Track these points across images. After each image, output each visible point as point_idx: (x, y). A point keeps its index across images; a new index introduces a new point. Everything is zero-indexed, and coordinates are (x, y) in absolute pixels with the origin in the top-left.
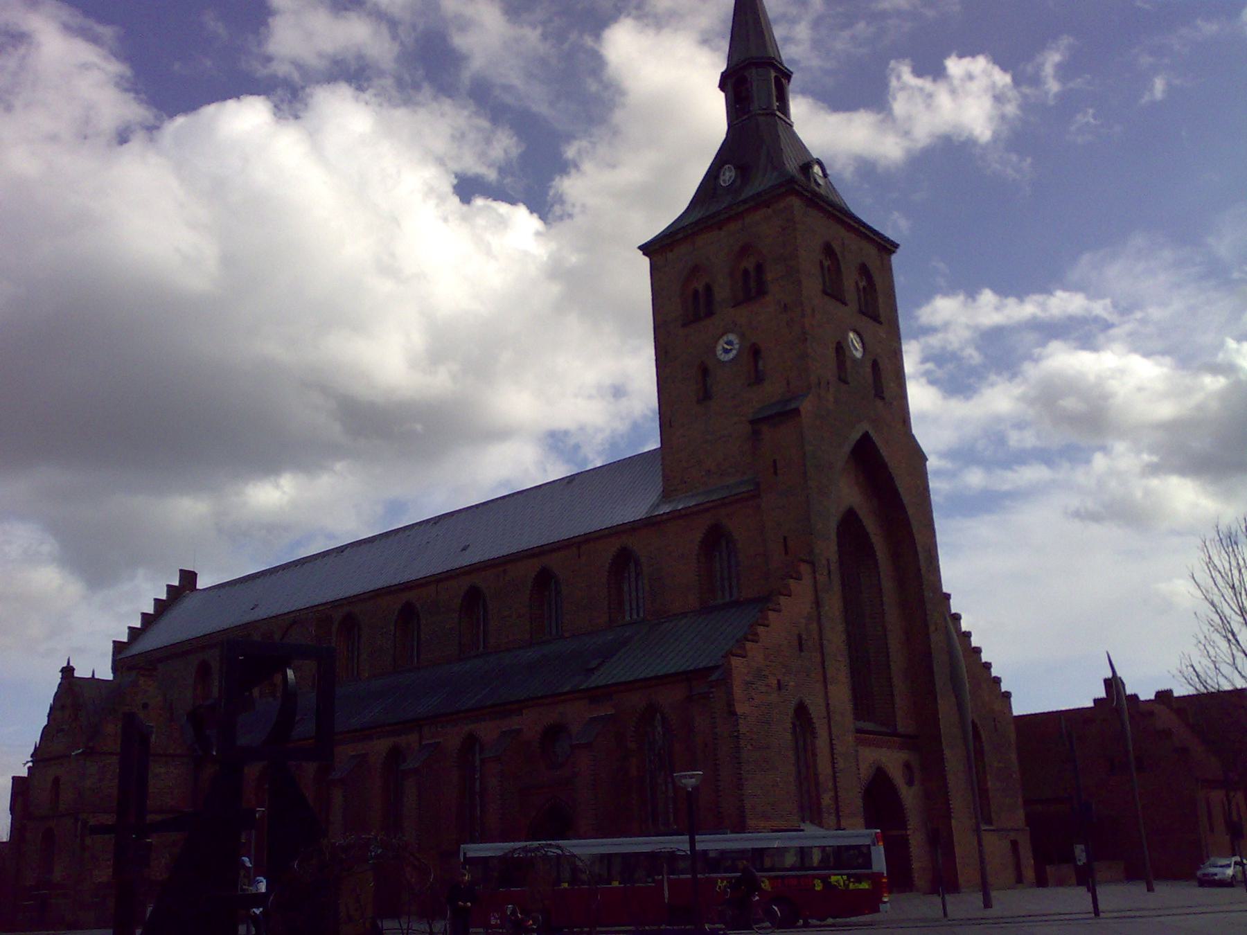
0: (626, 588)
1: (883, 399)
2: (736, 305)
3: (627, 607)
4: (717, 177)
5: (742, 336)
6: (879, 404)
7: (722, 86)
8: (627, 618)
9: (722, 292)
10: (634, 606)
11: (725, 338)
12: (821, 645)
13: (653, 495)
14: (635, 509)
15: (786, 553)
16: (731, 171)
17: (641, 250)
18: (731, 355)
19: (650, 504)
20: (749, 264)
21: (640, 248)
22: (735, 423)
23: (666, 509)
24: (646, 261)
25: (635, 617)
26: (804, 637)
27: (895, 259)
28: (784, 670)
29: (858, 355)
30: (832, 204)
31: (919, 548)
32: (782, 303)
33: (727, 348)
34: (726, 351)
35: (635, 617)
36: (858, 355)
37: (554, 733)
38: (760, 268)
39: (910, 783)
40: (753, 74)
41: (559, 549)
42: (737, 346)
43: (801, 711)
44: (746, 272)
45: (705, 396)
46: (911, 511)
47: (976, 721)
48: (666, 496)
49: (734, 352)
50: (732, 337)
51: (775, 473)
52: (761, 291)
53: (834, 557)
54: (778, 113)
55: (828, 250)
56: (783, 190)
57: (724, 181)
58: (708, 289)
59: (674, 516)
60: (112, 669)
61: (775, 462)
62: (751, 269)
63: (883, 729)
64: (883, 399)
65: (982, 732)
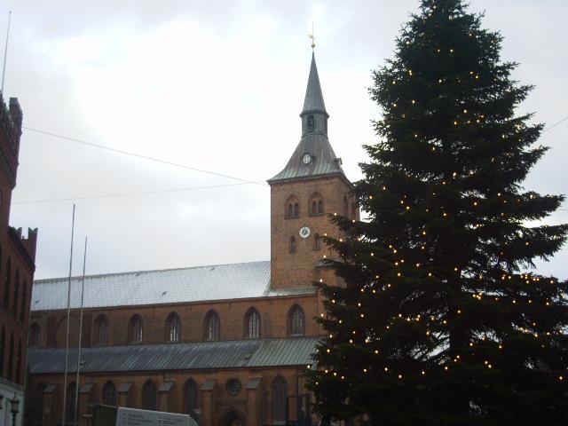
0: (250, 323)
3: (251, 331)
4: (302, 158)
5: (312, 229)
7: (302, 116)
8: (250, 336)
9: (304, 208)
18: (307, 235)
20: (316, 200)
23: (273, 294)
33: (305, 233)
37: (232, 383)
40: (316, 116)
45: (293, 250)
48: (273, 287)
58: (297, 205)
59: (277, 298)
62: (317, 202)
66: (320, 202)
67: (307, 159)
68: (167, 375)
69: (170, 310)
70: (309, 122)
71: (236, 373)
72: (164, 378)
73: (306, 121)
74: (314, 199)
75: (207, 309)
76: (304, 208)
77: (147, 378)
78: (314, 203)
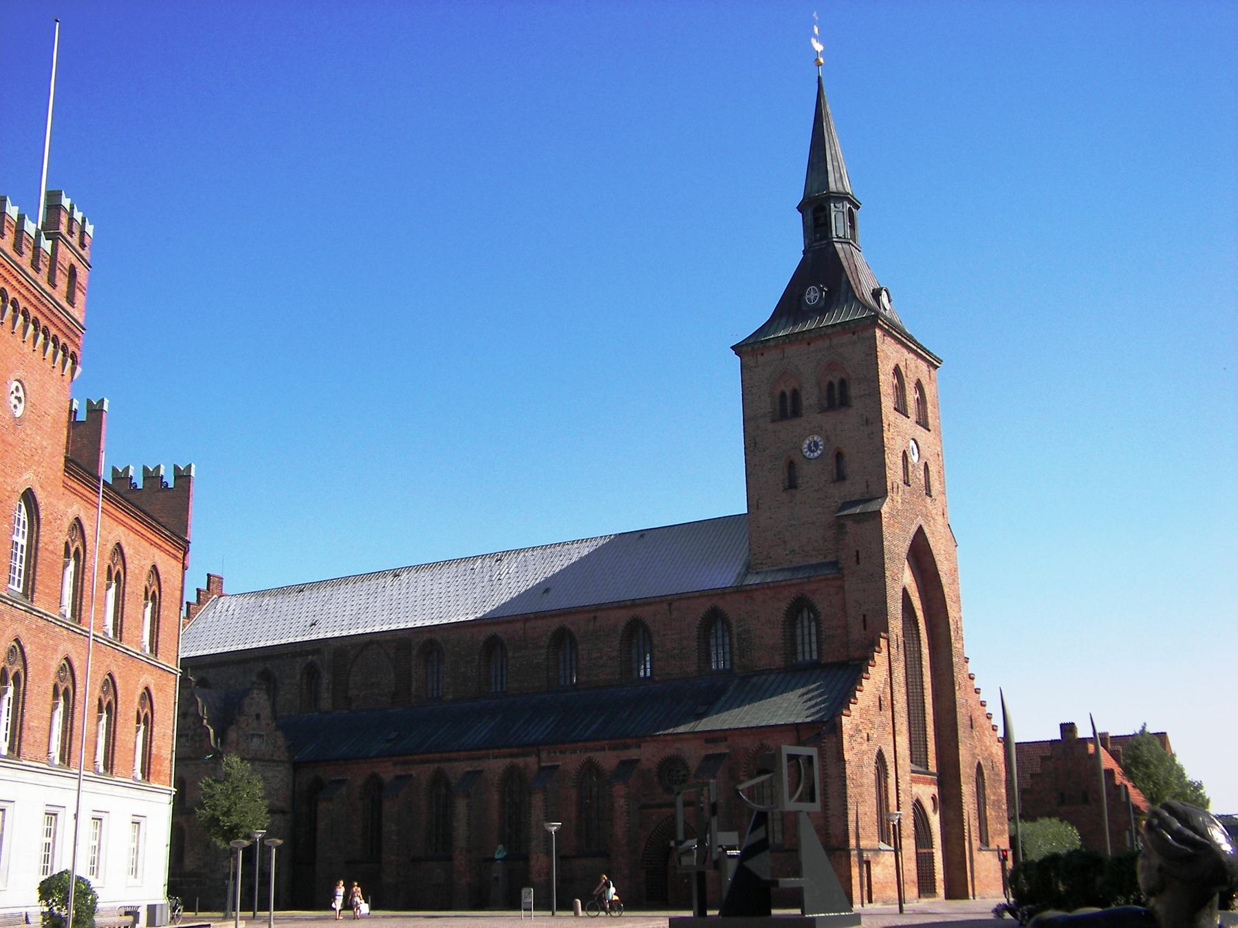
1: (931, 496)
2: (823, 410)
4: (802, 295)
5: (827, 440)
6: (928, 500)
9: (810, 397)
12: (892, 704)
13: (738, 568)
14: (723, 576)
15: (865, 629)
17: (733, 350)
19: (737, 572)
21: (732, 348)
22: (819, 513)
23: (753, 580)
26: (882, 698)
28: (870, 725)
31: (950, 620)
32: (864, 417)
38: (843, 383)
39: (935, 811)
41: (649, 604)
43: (880, 756)
46: (946, 590)
47: (982, 762)
48: (749, 569)
51: (858, 563)
53: (900, 634)
54: (851, 241)
55: (897, 371)
58: (796, 394)
59: (761, 587)
61: (857, 552)
63: (920, 769)
64: (931, 496)
65: (984, 771)
66: (843, 383)
68: (544, 755)
69: (555, 623)
70: (816, 219)
71: (678, 745)
72: (540, 761)
73: (810, 216)
74: (829, 378)
75: (623, 617)
76: (810, 397)
77: (508, 761)
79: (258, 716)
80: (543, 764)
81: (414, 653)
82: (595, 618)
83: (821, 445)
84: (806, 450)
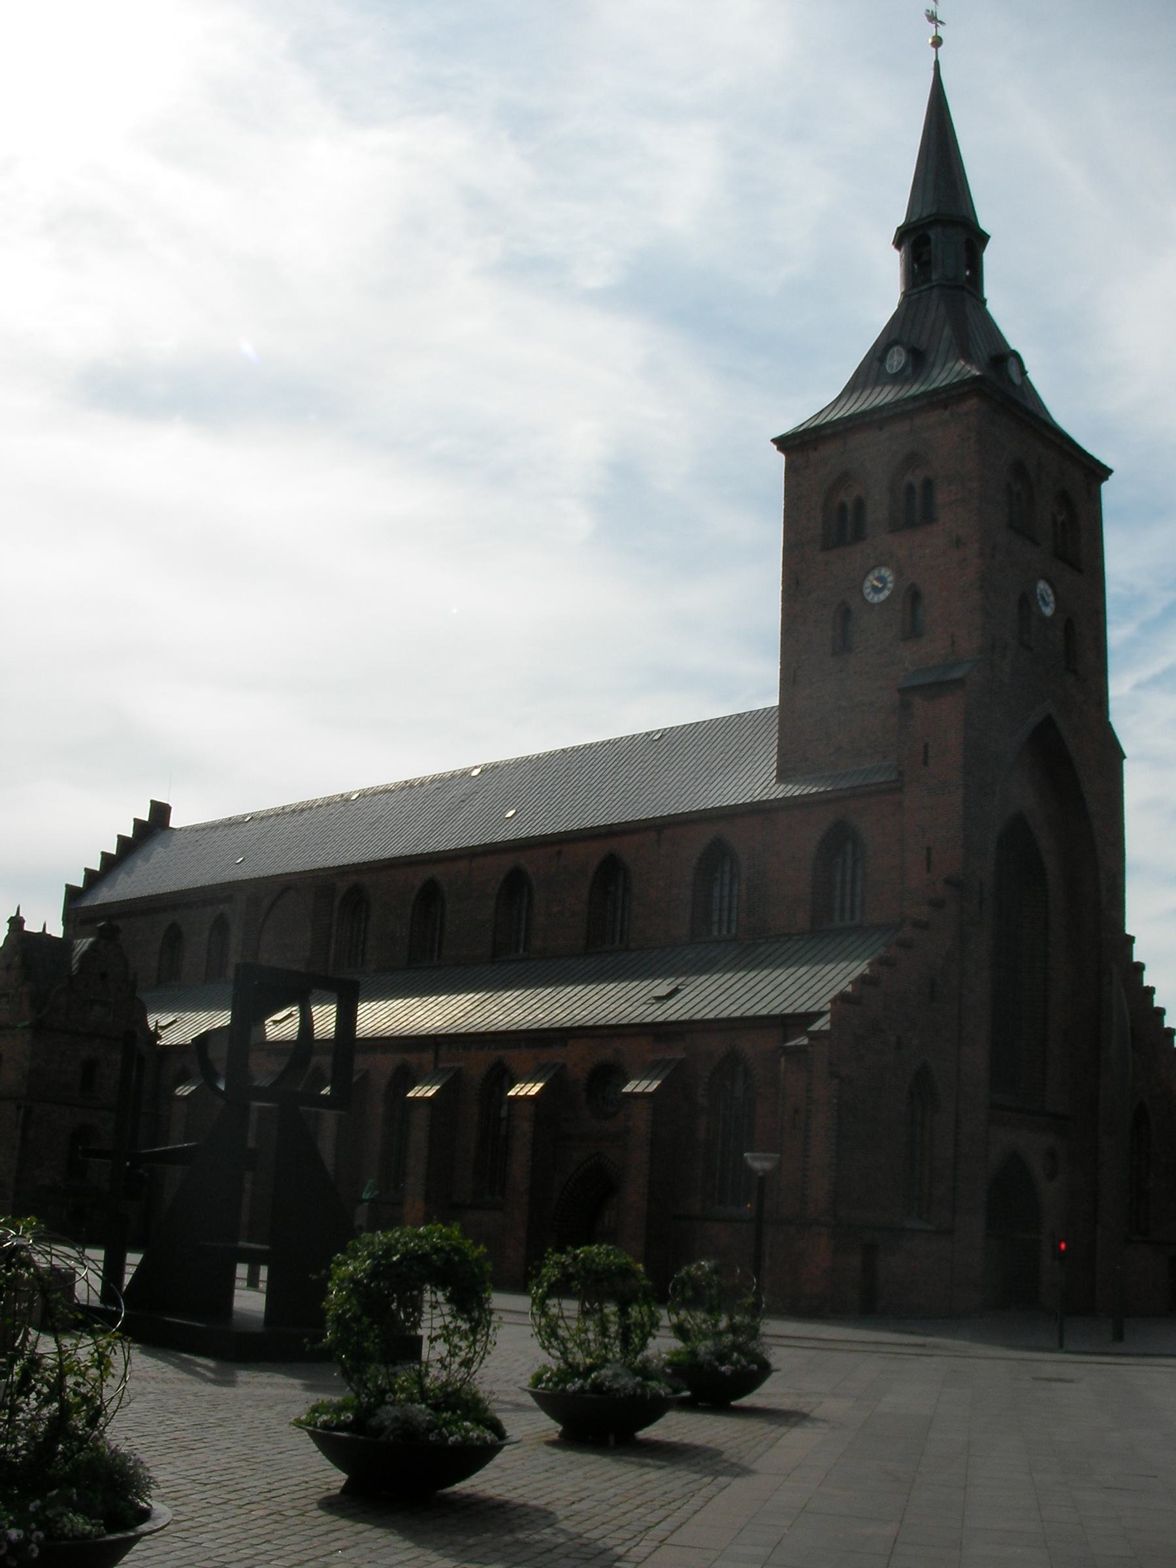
3: (715, 918)
5: (899, 573)
7: (898, 243)
8: (715, 933)
9: (878, 510)
10: (725, 918)
11: (876, 573)
15: (929, 870)
16: (900, 354)
18: (883, 596)
20: (916, 478)
21: (774, 441)
24: (780, 459)
25: (724, 932)
27: (1106, 488)
29: (1048, 611)
30: (1028, 412)
34: (877, 590)
35: (724, 932)
36: (1048, 611)
38: (928, 484)
42: (890, 585)
44: (910, 488)
45: (843, 646)
49: (886, 593)
50: (885, 572)
51: (925, 763)
52: (929, 517)
56: (966, 389)
57: (891, 366)
58: (860, 504)
60: (63, 919)
61: (926, 747)
66: (928, 484)
67: (896, 360)
72: (437, 1058)
76: (878, 510)
78: (910, 488)
79: (104, 976)
80: (441, 1065)
81: (337, 902)
82: (559, 853)
83: (891, 582)
84: (868, 590)
